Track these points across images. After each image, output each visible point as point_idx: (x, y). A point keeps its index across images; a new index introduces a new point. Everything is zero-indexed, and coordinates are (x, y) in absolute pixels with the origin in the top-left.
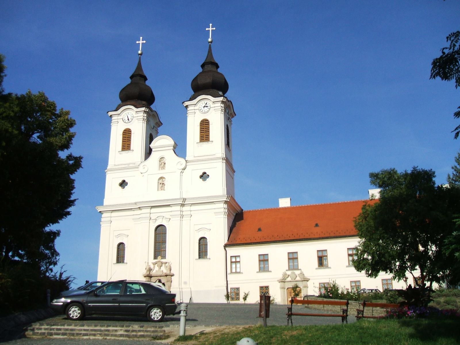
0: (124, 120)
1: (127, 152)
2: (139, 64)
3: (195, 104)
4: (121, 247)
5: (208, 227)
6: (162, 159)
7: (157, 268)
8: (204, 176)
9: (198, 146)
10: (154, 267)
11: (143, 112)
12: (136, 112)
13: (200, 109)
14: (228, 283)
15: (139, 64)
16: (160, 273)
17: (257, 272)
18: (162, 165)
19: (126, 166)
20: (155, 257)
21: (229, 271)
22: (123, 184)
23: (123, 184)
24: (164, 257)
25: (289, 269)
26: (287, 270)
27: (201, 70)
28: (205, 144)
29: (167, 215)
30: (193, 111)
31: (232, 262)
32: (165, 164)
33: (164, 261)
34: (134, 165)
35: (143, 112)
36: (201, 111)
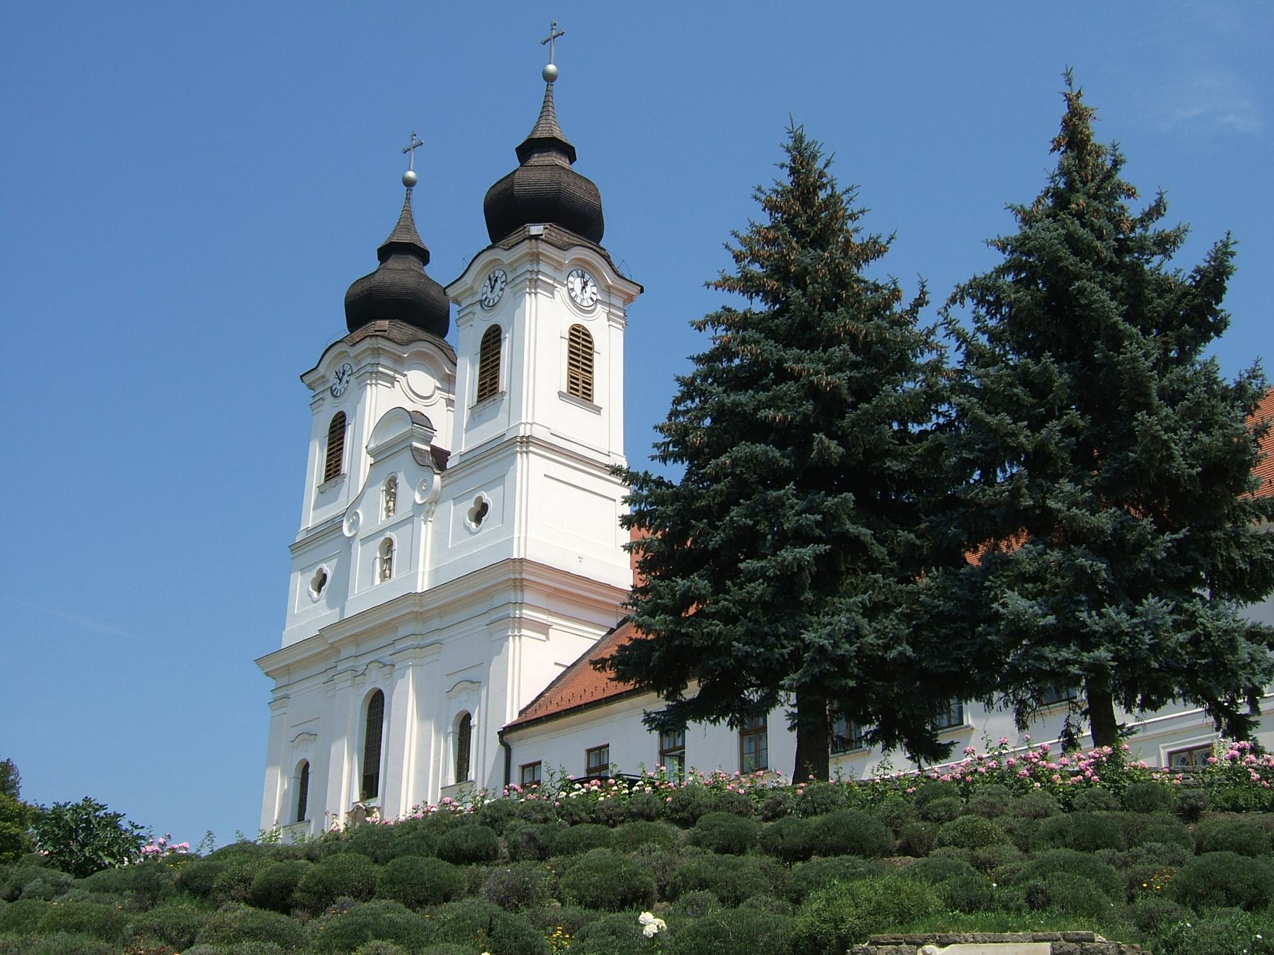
2: (407, 210)
3: (472, 288)
8: (480, 512)
11: (369, 352)
12: (356, 357)
15: (407, 210)
29: (385, 655)
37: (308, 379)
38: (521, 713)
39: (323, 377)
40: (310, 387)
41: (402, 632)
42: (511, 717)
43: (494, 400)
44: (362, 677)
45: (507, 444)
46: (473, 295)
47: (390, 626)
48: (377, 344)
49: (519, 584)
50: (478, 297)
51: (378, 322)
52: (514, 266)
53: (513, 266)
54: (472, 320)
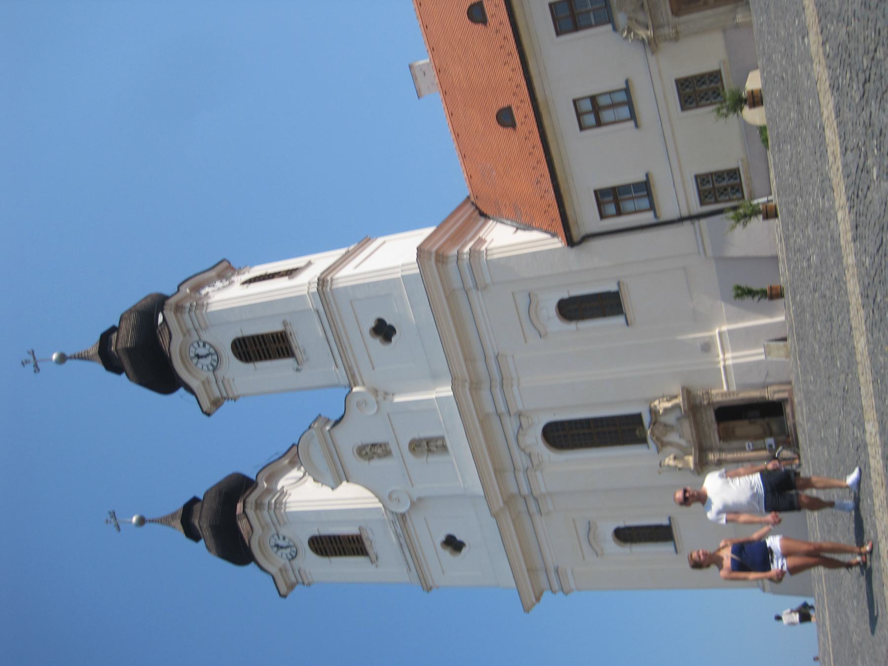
0: (291, 555)
1: (367, 544)
2: (165, 521)
4: (625, 535)
5: (523, 302)
6: (364, 453)
7: (673, 437)
9: (308, 359)
10: (670, 444)
12: (263, 528)
13: (211, 368)
14: (685, 213)
15: (165, 521)
16: (687, 427)
17: (637, 126)
18: (379, 451)
19: (402, 541)
20: (643, 441)
21: (647, 217)
22: (453, 544)
23: (453, 544)
24: (637, 419)
25: (610, 19)
26: (615, 29)
27: (124, 375)
28: (298, 341)
29: (511, 425)
30: (220, 383)
31: (619, 213)
32: (373, 445)
33: (646, 419)
34: (397, 522)
35: (258, 511)
36: (215, 364)
37: (283, 590)
38: (554, 235)
39: (281, 570)
40: (291, 587)
41: (489, 408)
42: (558, 243)
43: (291, 334)
44: (533, 457)
45: (323, 297)
46: (209, 382)
47: (484, 420)
48: (252, 503)
49: (441, 259)
50: (211, 375)
51: (238, 512)
52: (185, 330)
53: (186, 333)
54: (228, 381)
